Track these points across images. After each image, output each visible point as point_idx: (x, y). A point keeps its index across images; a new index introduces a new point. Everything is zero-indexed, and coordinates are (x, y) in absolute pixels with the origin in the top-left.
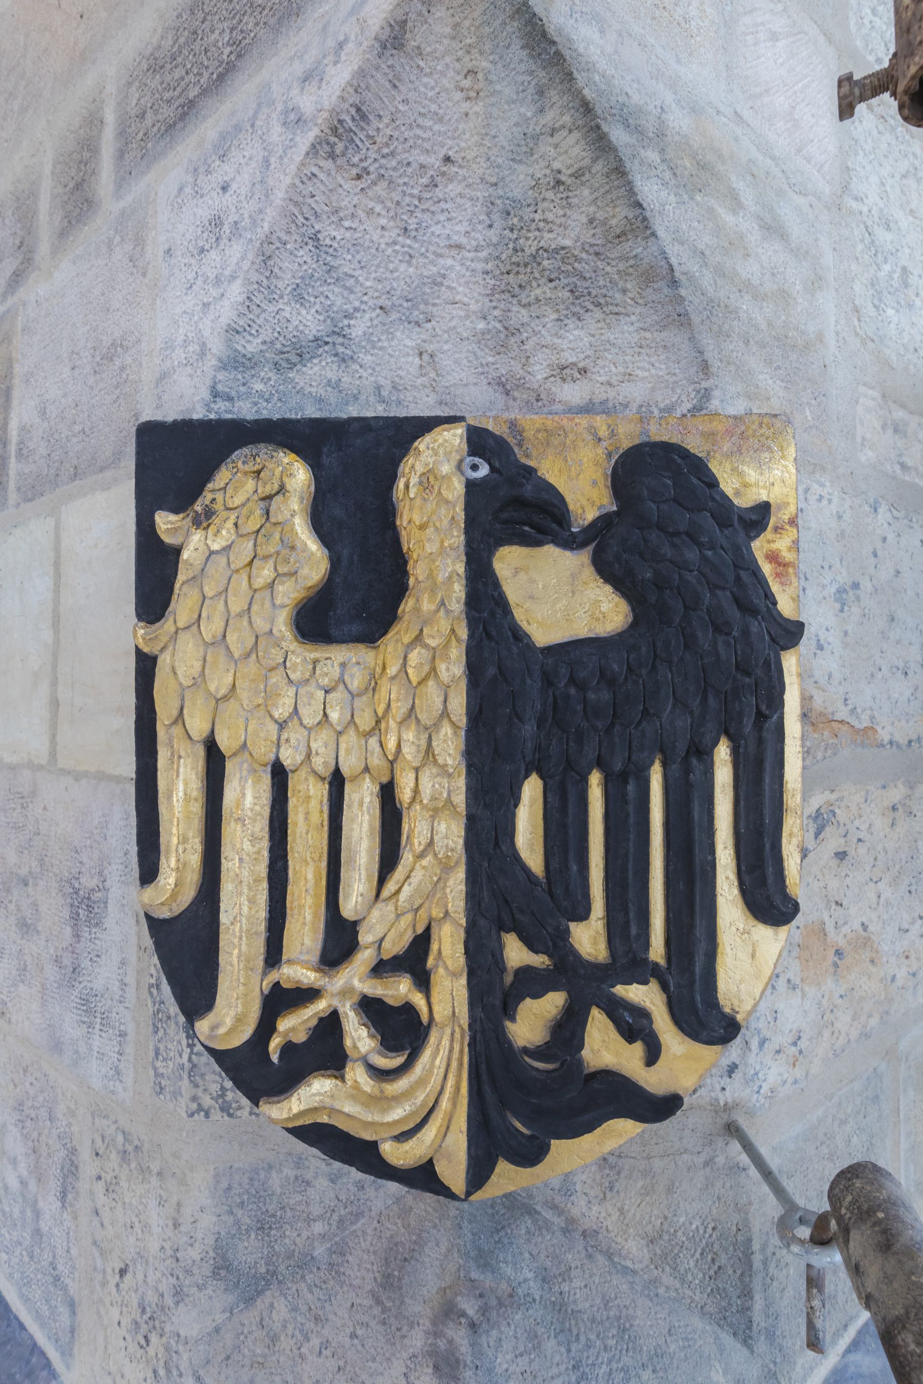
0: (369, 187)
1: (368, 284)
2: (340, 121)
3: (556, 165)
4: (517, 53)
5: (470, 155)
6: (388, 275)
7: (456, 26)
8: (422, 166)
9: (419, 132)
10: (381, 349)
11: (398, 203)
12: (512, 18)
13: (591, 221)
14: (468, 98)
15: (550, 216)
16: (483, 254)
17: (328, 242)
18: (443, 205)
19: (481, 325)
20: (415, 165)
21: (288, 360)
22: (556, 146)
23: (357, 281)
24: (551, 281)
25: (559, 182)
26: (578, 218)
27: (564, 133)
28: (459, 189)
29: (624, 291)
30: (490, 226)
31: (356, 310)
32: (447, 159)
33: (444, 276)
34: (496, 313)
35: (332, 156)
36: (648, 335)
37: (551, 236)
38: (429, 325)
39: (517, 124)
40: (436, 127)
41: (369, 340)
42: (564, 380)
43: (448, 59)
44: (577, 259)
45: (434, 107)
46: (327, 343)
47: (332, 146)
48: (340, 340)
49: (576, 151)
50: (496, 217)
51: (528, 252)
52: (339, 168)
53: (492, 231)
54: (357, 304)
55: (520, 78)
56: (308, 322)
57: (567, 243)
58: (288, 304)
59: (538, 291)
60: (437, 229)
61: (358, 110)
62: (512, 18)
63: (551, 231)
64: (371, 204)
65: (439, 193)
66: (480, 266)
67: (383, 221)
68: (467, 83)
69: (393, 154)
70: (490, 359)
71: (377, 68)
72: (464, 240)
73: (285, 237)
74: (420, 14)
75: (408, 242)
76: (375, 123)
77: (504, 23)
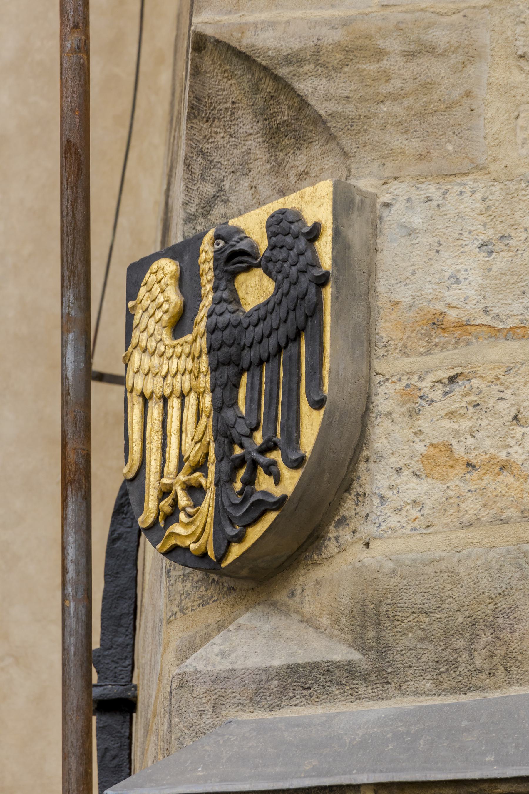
0: (212, 123)
1: (225, 163)
2: (193, 104)
3: (268, 90)
4: (235, 60)
5: (240, 98)
6: (232, 156)
7: (213, 60)
8: (226, 109)
9: (219, 97)
10: (237, 191)
11: (224, 126)
12: (227, 51)
13: (289, 107)
14: (229, 79)
15: (276, 110)
16: (260, 134)
17: (206, 151)
18: (239, 120)
19: (269, 166)
20: (224, 109)
21: (207, 211)
22: (265, 84)
23: (221, 164)
24: (286, 136)
25: (272, 96)
26: (284, 108)
27: (264, 79)
28: (242, 112)
29: (311, 131)
30: (258, 122)
31: (224, 177)
32: (233, 103)
33: (250, 149)
34: (273, 158)
35: (195, 117)
36: (323, 148)
37: (279, 117)
38: (251, 174)
39: (248, 82)
40: (224, 93)
41: (232, 189)
42: (302, 180)
43: (216, 71)
44: (292, 124)
45: (220, 87)
46: (218, 196)
47: (194, 113)
48: (222, 193)
49: (271, 83)
50: (259, 117)
51: (274, 127)
52: (199, 121)
53: (260, 124)
54: (224, 174)
55: (241, 67)
56: (209, 189)
57: (286, 118)
58: (201, 183)
59: (284, 143)
60: (241, 130)
61: (196, 98)
62: (227, 51)
63: (278, 116)
64: (216, 129)
65: (236, 116)
66: (261, 140)
67: (222, 135)
68: (226, 75)
69: (215, 108)
70: (276, 181)
71: (196, 83)
72: (251, 131)
73: (191, 155)
74: (200, 62)
75: (233, 139)
76: (204, 100)
77: (226, 54)
